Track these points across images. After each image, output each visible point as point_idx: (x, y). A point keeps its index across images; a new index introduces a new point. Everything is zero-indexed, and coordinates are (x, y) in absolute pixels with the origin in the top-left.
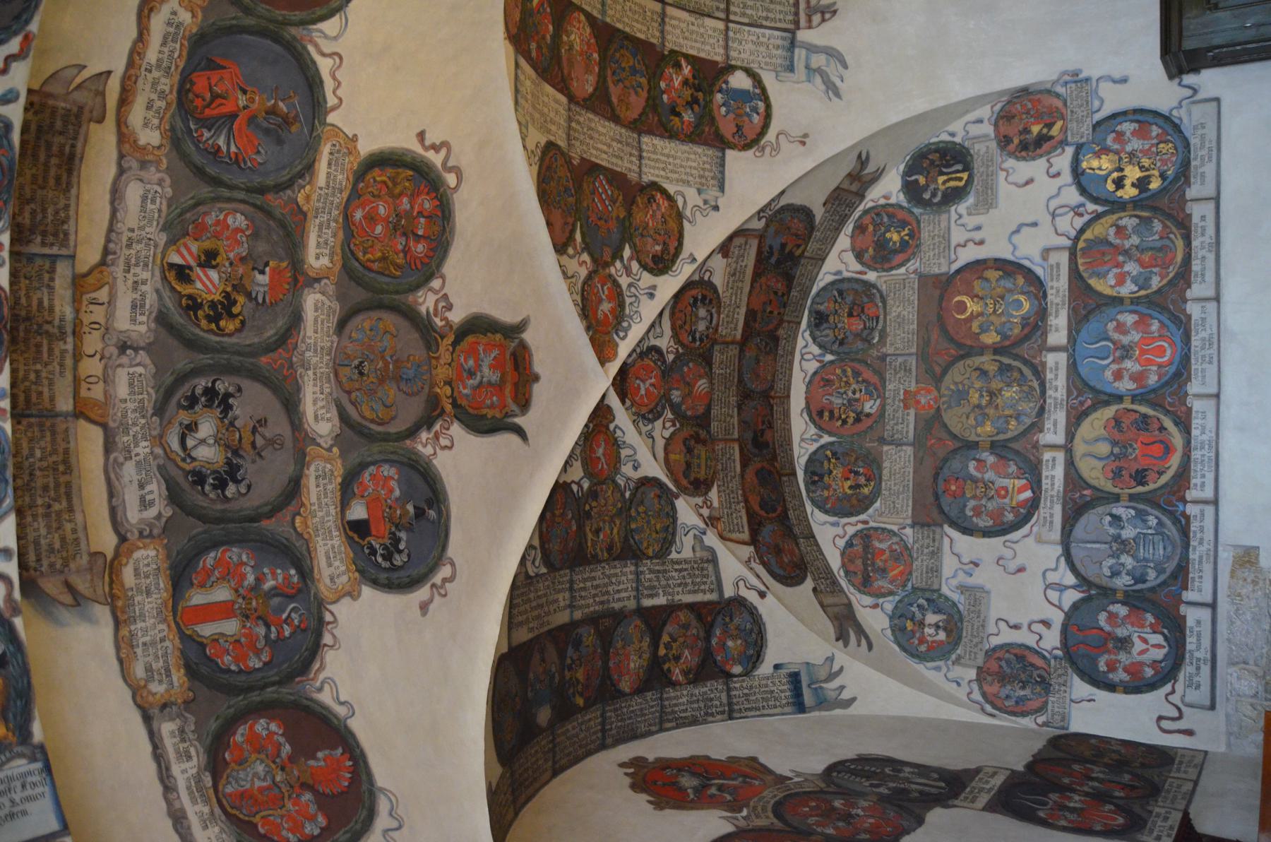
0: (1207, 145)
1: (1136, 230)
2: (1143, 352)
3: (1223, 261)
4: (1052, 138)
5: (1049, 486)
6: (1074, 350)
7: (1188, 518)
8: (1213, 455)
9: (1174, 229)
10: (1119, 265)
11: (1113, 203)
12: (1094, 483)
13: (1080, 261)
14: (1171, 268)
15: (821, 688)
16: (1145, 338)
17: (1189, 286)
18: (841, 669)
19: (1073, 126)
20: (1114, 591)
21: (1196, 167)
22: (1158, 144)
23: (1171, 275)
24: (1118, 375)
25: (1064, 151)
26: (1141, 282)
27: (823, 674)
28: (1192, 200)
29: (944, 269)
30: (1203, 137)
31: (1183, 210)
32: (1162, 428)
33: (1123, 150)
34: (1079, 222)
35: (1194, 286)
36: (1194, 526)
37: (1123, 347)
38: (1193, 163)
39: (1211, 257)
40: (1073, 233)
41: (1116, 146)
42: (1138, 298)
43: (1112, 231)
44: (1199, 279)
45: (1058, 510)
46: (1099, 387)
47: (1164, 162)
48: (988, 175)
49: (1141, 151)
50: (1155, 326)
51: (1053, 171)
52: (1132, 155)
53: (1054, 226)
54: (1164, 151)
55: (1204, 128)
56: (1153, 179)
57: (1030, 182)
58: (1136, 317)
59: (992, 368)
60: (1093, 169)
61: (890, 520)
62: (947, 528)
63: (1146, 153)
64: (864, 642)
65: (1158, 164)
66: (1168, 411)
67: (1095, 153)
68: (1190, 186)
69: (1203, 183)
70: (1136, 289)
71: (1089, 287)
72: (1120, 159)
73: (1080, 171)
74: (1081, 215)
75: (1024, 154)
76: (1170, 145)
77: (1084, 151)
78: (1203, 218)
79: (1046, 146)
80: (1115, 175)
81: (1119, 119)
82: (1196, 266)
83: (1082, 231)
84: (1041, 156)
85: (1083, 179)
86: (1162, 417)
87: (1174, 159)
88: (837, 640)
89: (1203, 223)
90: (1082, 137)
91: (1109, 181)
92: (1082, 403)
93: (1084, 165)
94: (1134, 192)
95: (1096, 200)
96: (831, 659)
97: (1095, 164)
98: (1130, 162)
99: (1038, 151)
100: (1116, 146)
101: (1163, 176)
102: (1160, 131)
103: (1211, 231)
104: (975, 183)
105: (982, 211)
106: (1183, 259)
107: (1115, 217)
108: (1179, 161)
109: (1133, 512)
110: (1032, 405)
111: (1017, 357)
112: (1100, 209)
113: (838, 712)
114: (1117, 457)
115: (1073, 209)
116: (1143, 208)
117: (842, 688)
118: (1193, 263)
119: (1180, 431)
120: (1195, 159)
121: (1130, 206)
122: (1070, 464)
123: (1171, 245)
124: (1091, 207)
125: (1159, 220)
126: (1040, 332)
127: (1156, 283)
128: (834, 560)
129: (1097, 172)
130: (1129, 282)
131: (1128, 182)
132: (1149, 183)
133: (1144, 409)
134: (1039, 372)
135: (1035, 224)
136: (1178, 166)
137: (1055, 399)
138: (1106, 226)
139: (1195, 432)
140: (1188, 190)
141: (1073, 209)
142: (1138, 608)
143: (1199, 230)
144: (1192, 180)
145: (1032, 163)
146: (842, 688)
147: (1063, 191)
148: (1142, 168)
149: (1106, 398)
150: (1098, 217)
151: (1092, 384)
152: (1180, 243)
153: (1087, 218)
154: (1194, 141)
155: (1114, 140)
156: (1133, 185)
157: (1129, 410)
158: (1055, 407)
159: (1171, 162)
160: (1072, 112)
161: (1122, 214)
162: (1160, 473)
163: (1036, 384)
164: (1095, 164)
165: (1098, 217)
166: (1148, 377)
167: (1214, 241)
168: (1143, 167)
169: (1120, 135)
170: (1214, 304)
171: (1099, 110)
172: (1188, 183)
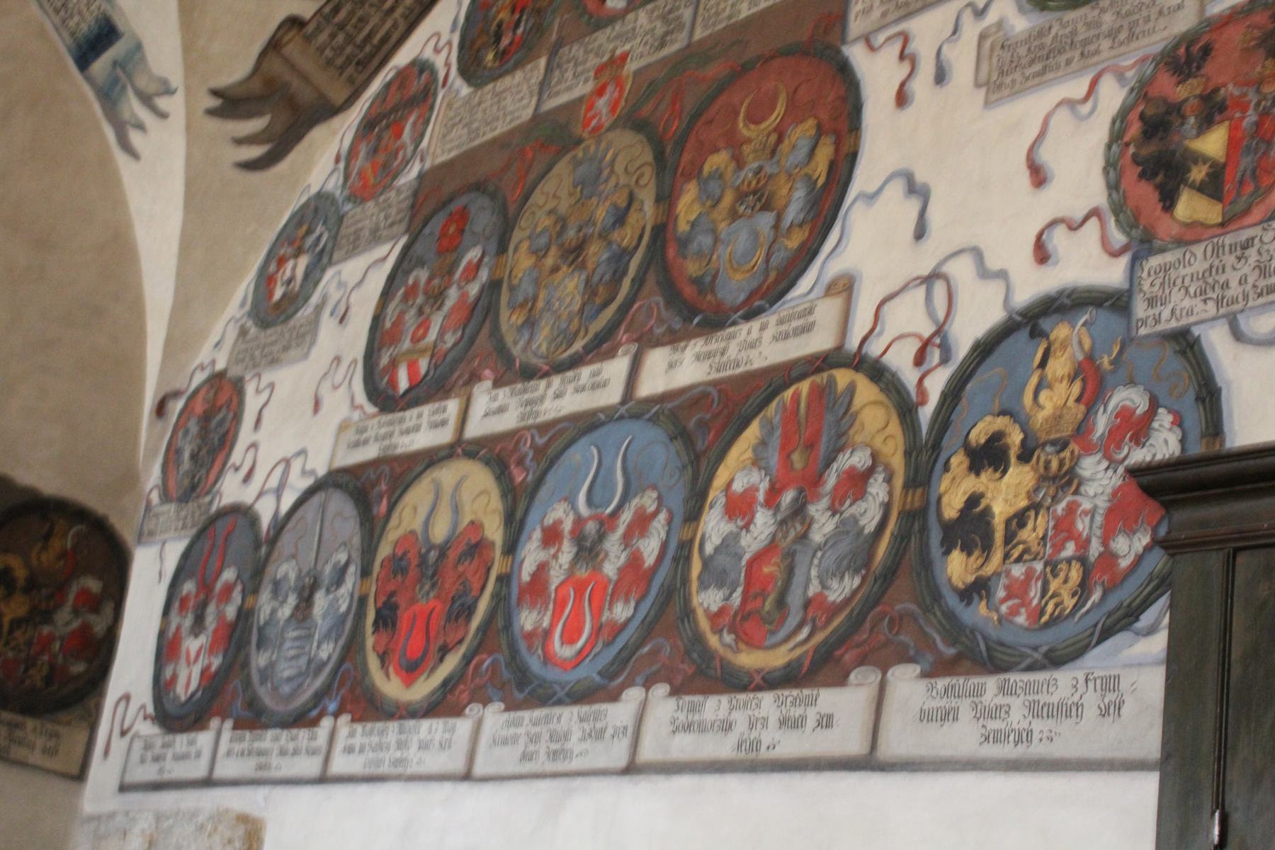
0: (1038, 726)
1: (847, 528)
2: (580, 589)
3: (712, 782)
4: (1168, 200)
5: (405, 426)
6: (621, 418)
7: (315, 723)
8: (385, 769)
9: (819, 637)
10: (772, 499)
11: (936, 446)
12: (394, 521)
13: (804, 387)
14: (728, 638)
15: (124, 88)
16: (606, 588)
17: (676, 692)
18: (163, 115)
19: (1198, 259)
20: (256, 591)
21: (979, 692)
22: (1082, 560)
23: (713, 641)
24: (551, 536)
25: (1115, 254)
26: (722, 560)
27: (142, 82)
28: (882, 687)
29: (856, 26)
30: (1070, 710)
31: (862, 661)
32: (444, 651)
33: (1088, 449)
34: (901, 361)
35: (672, 703)
36: (303, 734)
37: (601, 537)
38: (991, 683)
39: (723, 748)
40: (874, 349)
41: (1102, 423)
42: (688, 559)
43: (858, 459)
44: (682, 717)
45: (370, 453)
46: (543, 493)
47: (1018, 591)
48: (1086, 42)
49: (1072, 509)
50: (621, 611)
51: (1059, 240)
52: (1067, 480)
53: (904, 288)
54: (1054, 586)
55: (1104, 713)
56: (976, 559)
57: (1038, 176)
58: (649, 560)
59: (625, 236)
60: (1043, 364)
61: (437, 128)
62: (403, 241)
63: (1064, 527)
64: (255, 152)
65: (1018, 571)
66: (468, 663)
67: (1090, 358)
68: (925, 675)
69: (926, 716)
70: (709, 549)
71: (745, 424)
72: (1062, 445)
73: (1045, 324)
74: (919, 359)
75: (1135, 129)
76: (1069, 603)
77: (1104, 318)
78: (826, 722)
79: (1146, 194)
80: (1015, 438)
81: (1195, 418)
82: (715, 706)
83: (877, 372)
84: (1113, 187)
85: (1023, 335)
86: (462, 649)
87: (1021, 619)
88: (215, 93)
89: (811, 722)
90: (1151, 302)
91: (1001, 423)
92: (520, 462)
93: (1061, 331)
94: (952, 506)
95: (953, 394)
96: (169, 91)
97: (1059, 366)
98: (1045, 478)
99: (1133, 172)
100: (1102, 423)
101: (978, 589)
102: (1124, 563)
103: (790, 745)
104: (1071, 15)
105: (985, 68)
106: (740, 669)
107: (898, 462)
108: (1007, 636)
109: (343, 608)
110: (544, 348)
111: (639, 282)
112: (926, 413)
113: (110, 133)
114: (423, 559)
115: (940, 331)
116: (902, 539)
117: (140, 127)
118: (724, 699)
119: (433, 693)
120: (1003, 690)
121: (915, 500)
122: (432, 458)
123: (782, 634)
124: (937, 384)
125: (854, 593)
126: (677, 324)
127: (708, 600)
128: (402, 58)
129: (1034, 380)
130: (727, 527)
131: (984, 482)
132: (968, 550)
133: (483, 605)
134: (600, 348)
135: (920, 232)
136: (993, 633)
137: (542, 399)
138: (878, 442)
139: (425, 724)
140: (915, 669)
141: (940, 331)
142: (231, 636)
143: (797, 712)
144: (942, 683)
145: (1099, 162)
146: (140, 127)
147: (994, 291)
148: (1019, 519)
149: (519, 514)
150: (906, 408)
151: (551, 478)
152: (777, 658)
153: (909, 376)
154: (1064, 681)
155: (1125, 415)
156: (974, 500)
157: (488, 570)
158: (529, 403)
159: (1014, 612)
160: (1247, 245)
161: (899, 482)
162: (383, 658)
163: (578, 346)
164: (1059, 366)
165: (906, 408)
166: (533, 606)
167: (764, 754)
168: (1022, 525)
169: (1138, 428)
170: (622, 762)
171: (1238, 335)
172: (938, 668)
